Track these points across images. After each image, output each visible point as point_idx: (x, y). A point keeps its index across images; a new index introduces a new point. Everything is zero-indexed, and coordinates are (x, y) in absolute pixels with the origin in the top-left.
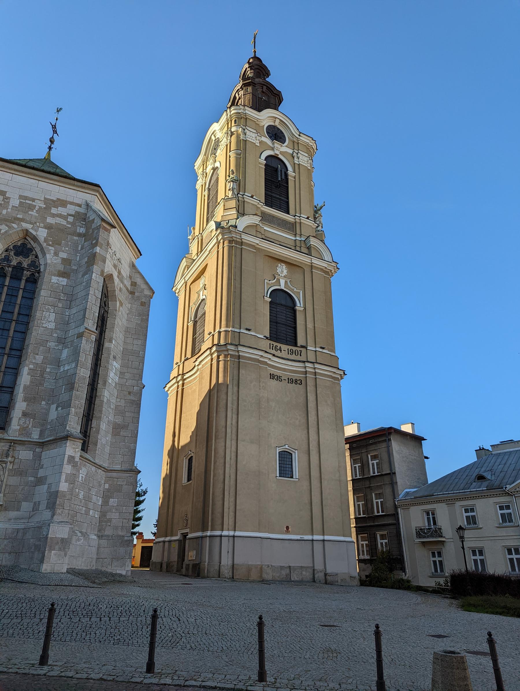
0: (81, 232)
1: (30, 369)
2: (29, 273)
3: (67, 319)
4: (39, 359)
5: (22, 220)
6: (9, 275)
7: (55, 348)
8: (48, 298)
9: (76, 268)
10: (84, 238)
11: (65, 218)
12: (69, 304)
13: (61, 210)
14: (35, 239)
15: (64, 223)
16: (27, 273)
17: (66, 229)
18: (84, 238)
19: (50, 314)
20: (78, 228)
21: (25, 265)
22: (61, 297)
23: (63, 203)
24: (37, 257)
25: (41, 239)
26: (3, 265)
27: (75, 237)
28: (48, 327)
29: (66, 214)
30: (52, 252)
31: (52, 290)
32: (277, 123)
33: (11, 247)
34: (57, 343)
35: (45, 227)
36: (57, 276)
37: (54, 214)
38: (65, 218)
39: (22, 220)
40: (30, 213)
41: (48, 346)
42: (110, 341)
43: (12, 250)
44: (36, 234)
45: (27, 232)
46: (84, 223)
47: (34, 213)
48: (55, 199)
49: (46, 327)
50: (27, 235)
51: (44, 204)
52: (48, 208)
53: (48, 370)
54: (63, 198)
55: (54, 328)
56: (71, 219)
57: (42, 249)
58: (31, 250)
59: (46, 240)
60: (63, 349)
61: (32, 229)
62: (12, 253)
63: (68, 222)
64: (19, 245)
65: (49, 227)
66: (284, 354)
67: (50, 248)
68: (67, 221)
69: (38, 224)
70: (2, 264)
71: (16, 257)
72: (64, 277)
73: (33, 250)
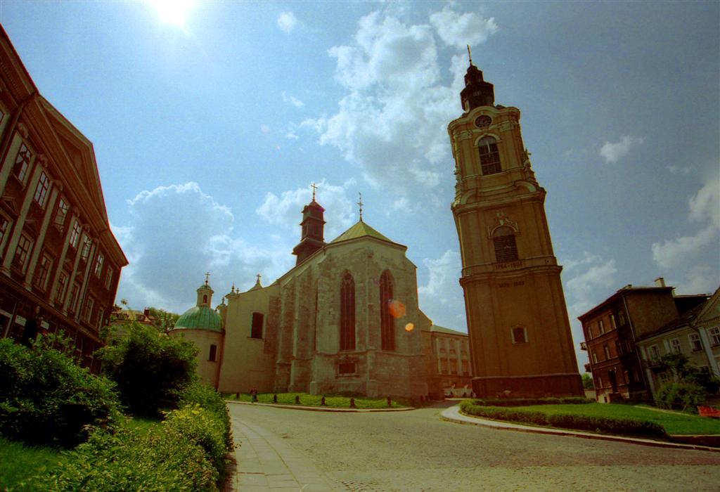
32: (482, 114)
66: (509, 269)
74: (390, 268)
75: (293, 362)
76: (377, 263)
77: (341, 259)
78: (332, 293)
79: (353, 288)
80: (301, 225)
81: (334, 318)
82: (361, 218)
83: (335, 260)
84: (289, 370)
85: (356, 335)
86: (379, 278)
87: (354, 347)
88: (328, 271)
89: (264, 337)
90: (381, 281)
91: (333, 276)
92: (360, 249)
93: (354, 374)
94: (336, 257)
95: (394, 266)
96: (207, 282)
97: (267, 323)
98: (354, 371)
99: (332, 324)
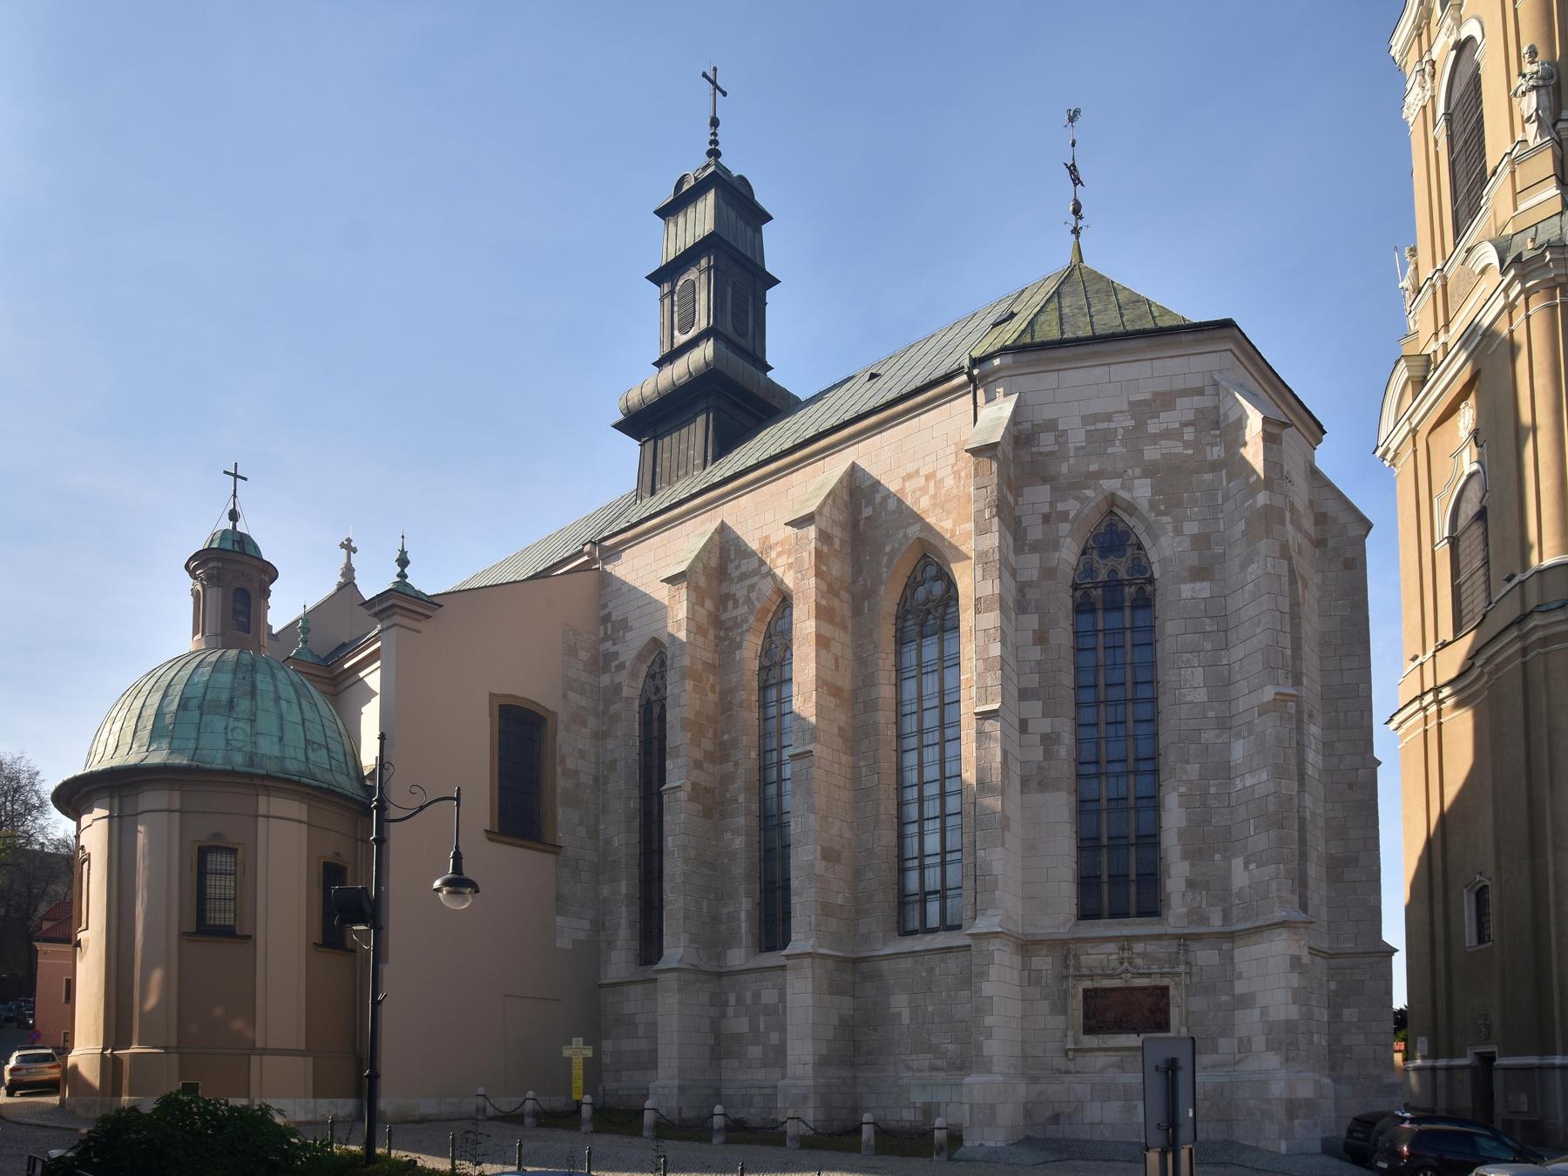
0: (1215, 457)
1: (1181, 795)
2: (1133, 589)
3: (1226, 674)
4: (1193, 770)
5: (1099, 475)
6: (1099, 605)
7: (1218, 741)
8: (1183, 636)
9: (1222, 551)
10: (1224, 471)
11: (1174, 435)
12: (1224, 638)
13: (1169, 420)
14: (1131, 509)
15: (1178, 448)
16: (1131, 590)
17: (1184, 461)
18: (1224, 471)
19: (1194, 669)
20: (1208, 448)
21: (1123, 574)
22: (1207, 627)
23: (1165, 400)
24: (1140, 546)
25: (1143, 505)
26: (1085, 588)
27: (1205, 476)
28: (1195, 701)
29: (1177, 425)
30: (1169, 527)
31: (1186, 616)
33: (1091, 542)
34: (1218, 731)
35: (1145, 475)
36: (1190, 582)
37: (1155, 435)
38: (1174, 435)
39: (1099, 475)
40: (1110, 450)
41: (1203, 741)
43: (1094, 548)
44: (1133, 498)
45: (1112, 500)
46: (1218, 432)
47: (1117, 449)
48: (1148, 396)
49: (1192, 702)
50: (1113, 504)
51: (1132, 419)
52: (1140, 425)
53: (1213, 790)
54: (1162, 386)
55: (1206, 699)
56: (1189, 434)
57: (1149, 528)
58: (1128, 532)
59: (1153, 505)
60: (1232, 740)
61: (1123, 487)
62: (1095, 556)
63: (1186, 445)
64: (1103, 531)
65: (1150, 471)
67: (1166, 519)
68: (1183, 442)
69: (1130, 471)
70: (1083, 586)
71: (1104, 561)
72: (1203, 579)
73: (1130, 532)
77: (1077, 438)
92: (1186, 393)
94: (1051, 425)
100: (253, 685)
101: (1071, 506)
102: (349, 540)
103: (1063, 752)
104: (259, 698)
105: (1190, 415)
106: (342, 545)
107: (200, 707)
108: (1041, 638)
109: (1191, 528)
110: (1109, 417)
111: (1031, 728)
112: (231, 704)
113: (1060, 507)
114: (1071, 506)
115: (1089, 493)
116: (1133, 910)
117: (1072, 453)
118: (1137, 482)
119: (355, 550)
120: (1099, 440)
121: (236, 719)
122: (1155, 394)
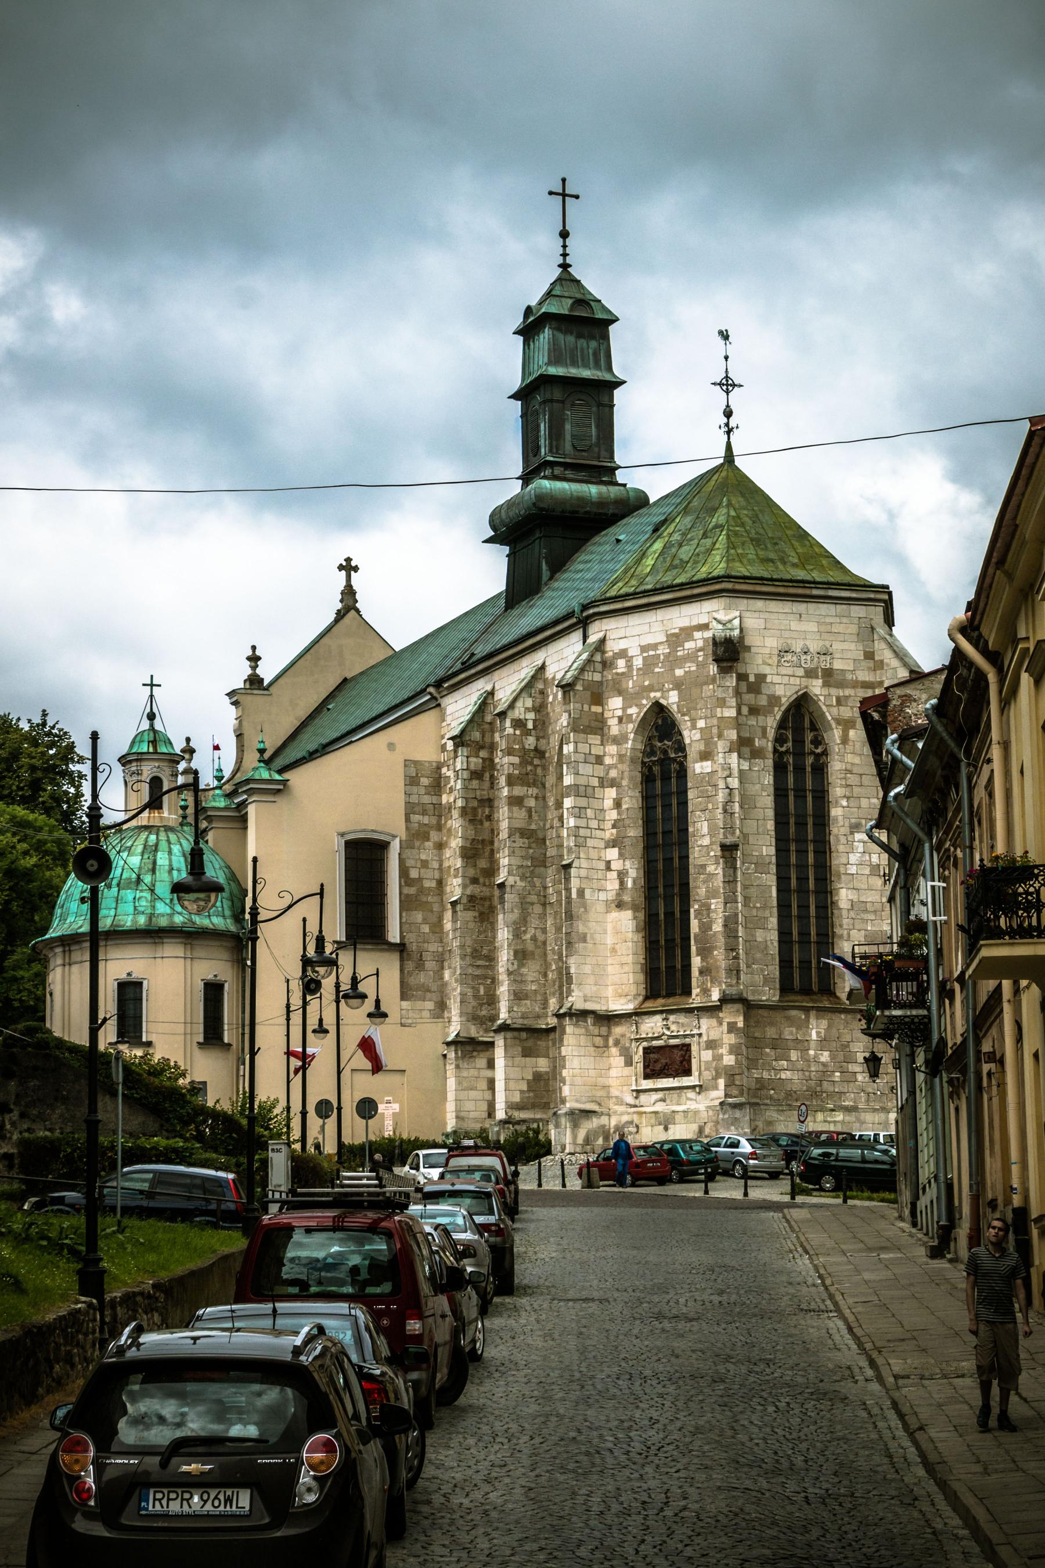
23: (687, 633)
42: (837, 804)
48: (677, 631)
65: (678, 685)
67: (687, 718)
74: (816, 687)
75: (500, 1042)
76: (761, 678)
77: (638, 662)
78: (611, 793)
79: (682, 773)
80: (515, 396)
81: (622, 883)
82: (729, 447)
83: (621, 663)
84: (491, 1065)
85: (693, 949)
86: (771, 734)
87: (688, 993)
88: (596, 709)
89: (394, 935)
90: (779, 740)
91: (615, 729)
93: (686, 1081)
94: (623, 654)
95: (829, 676)
96: (151, 717)
97: (404, 872)
98: (688, 1072)
99: (620, 905)
100: (154, 863)
101: (633, 710)
102: (348, 560)
103: (630, 884)
104: (157, 873)
105: (700, 644)
106: (341, 568)
107: (118, 885)
108: (618, 804)
109: (701, 724)
110: (655, 647)
111: (614, 866)
112: (139, 880)
113: (630, 711)
114: (633, 710)
115: (644, 702)
116: (664, 993)
117: (635, 673)
118: (672, 693)
119: (356, 569)
120: (649, 663)
121: (142, 891)
122: (681, 629)
